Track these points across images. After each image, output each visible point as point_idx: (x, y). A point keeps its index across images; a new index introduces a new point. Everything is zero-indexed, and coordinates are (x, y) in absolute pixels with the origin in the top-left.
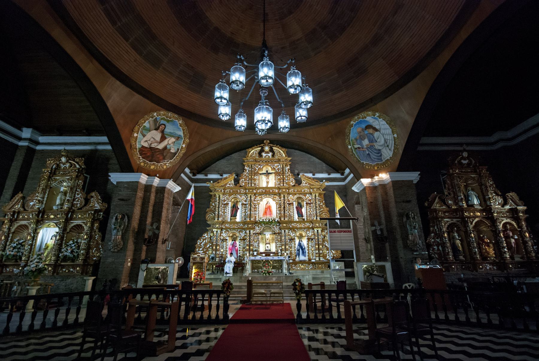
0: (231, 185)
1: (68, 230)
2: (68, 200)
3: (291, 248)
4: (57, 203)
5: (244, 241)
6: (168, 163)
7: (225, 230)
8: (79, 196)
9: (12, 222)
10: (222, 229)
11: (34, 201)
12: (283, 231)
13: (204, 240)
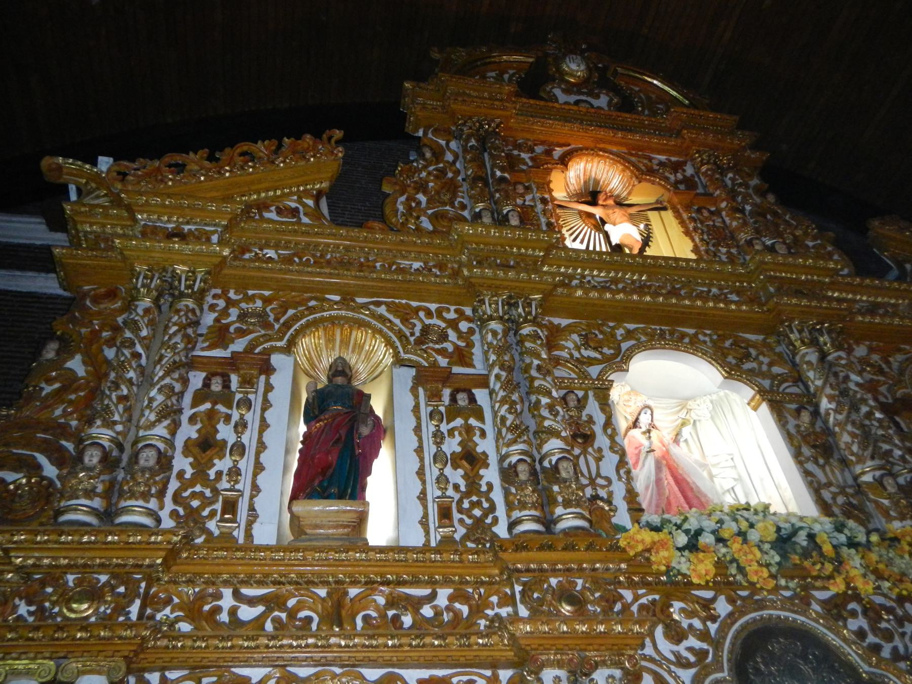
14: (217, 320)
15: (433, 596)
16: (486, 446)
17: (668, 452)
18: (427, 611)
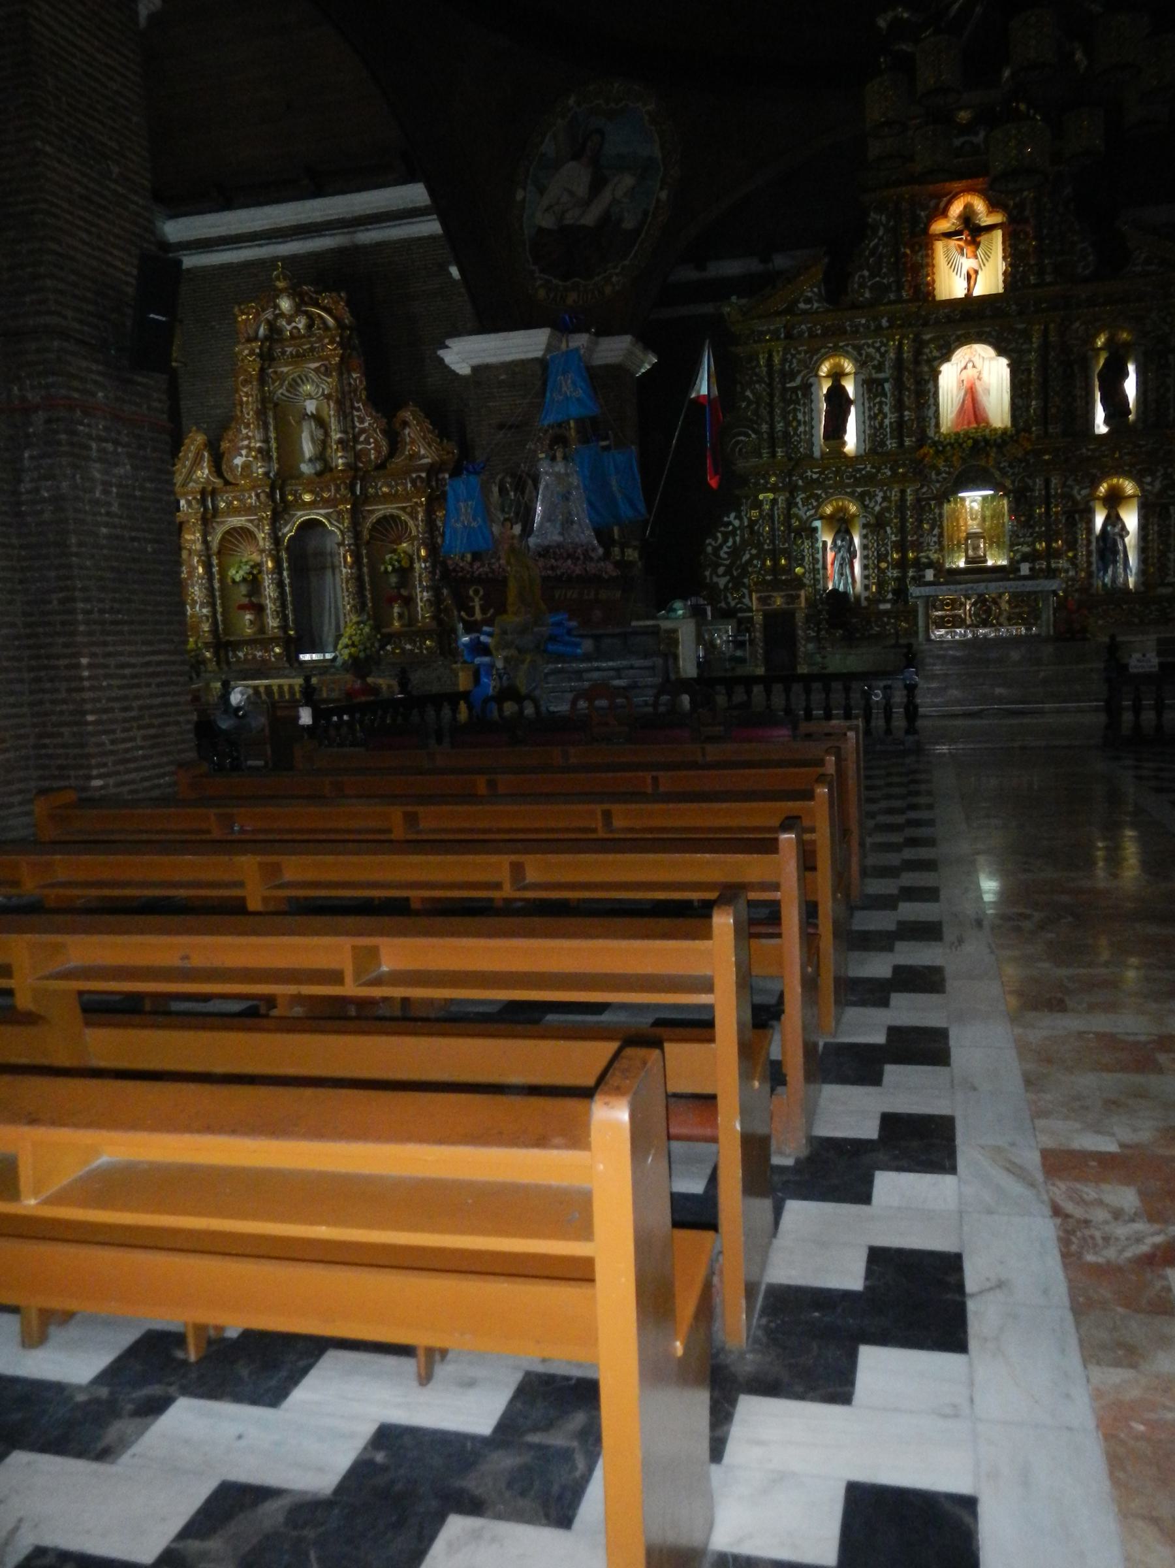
0: (816, 305)
1: (366, 535)
2: (340, 441)
3: (1072, 545)
4: (307, 455)
5: (882, 532)
6: (617, 275)
7: (804, 492)
8: (366, 421)
9: (207, 520)
11: (244, 452)
12: (1039, 482)
13: (726, 536)
14: (789, 366)
15: (866, 467)
16: (886, 409)
17: (974, 383)
18: (864, 472)
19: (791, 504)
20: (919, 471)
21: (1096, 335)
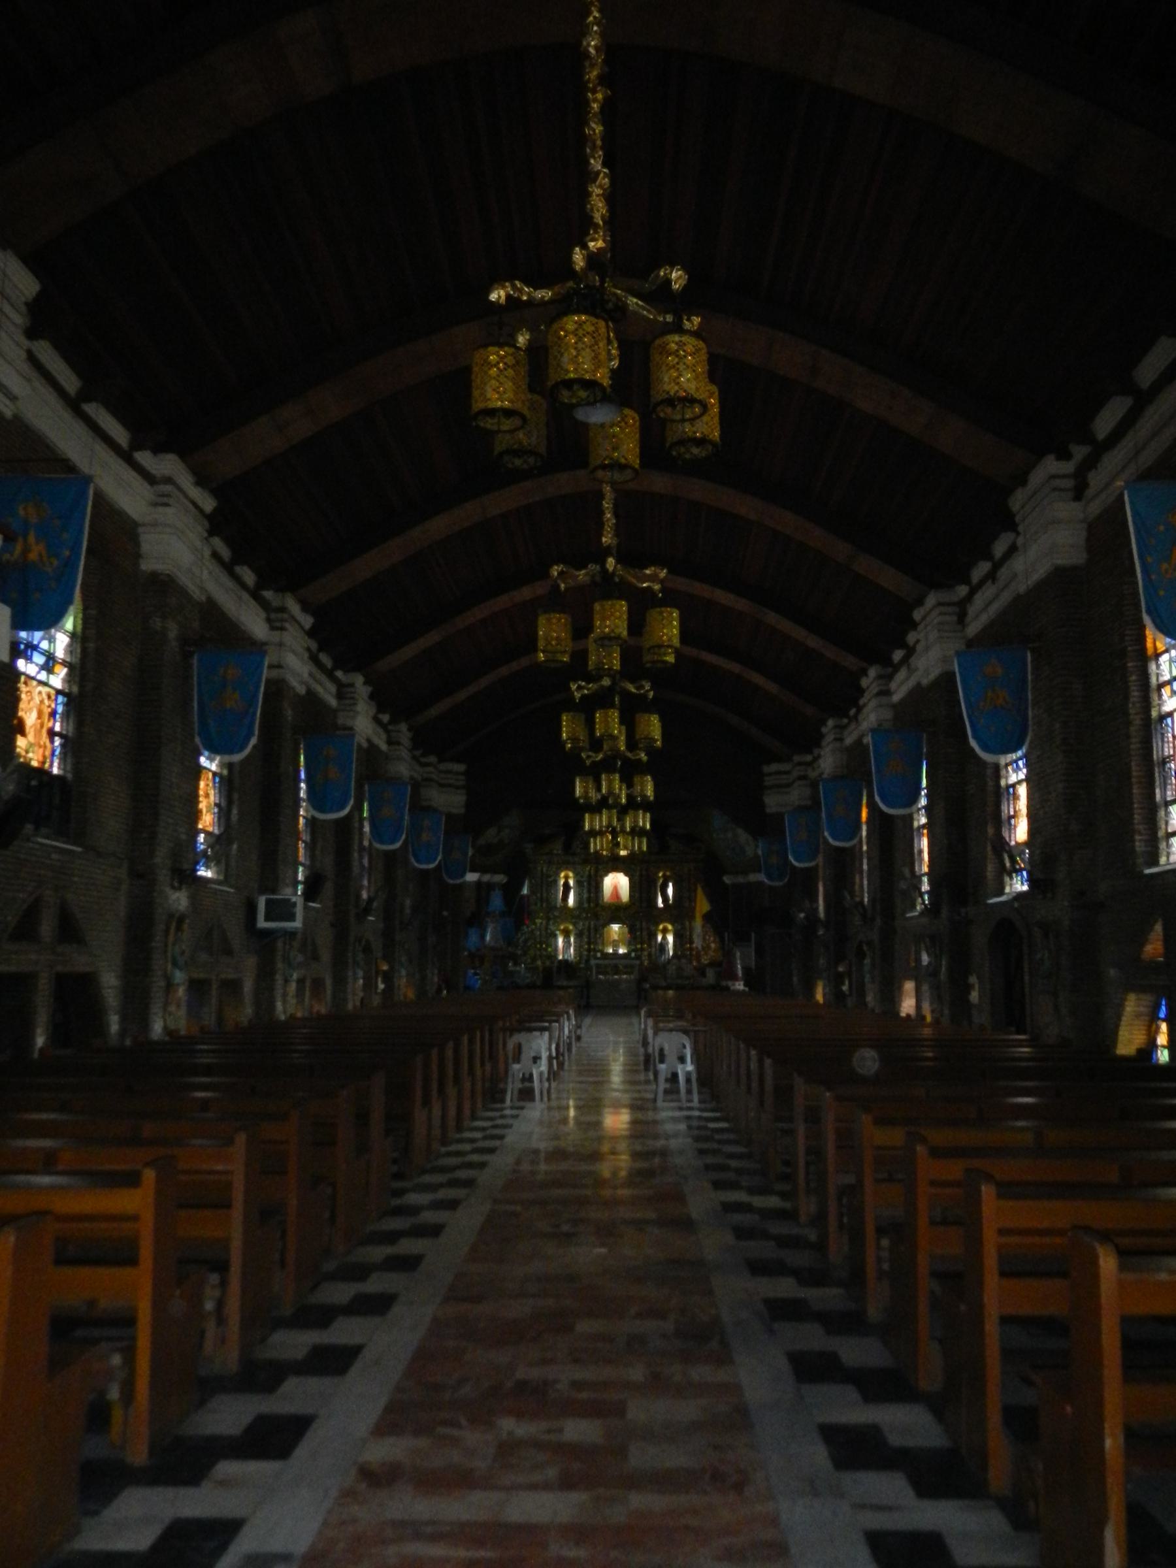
3: (650, 946)
10: (548, 919)
13: (522, 934)
19: (547, 924)
20: (596, 916)
21: (659, 872)
